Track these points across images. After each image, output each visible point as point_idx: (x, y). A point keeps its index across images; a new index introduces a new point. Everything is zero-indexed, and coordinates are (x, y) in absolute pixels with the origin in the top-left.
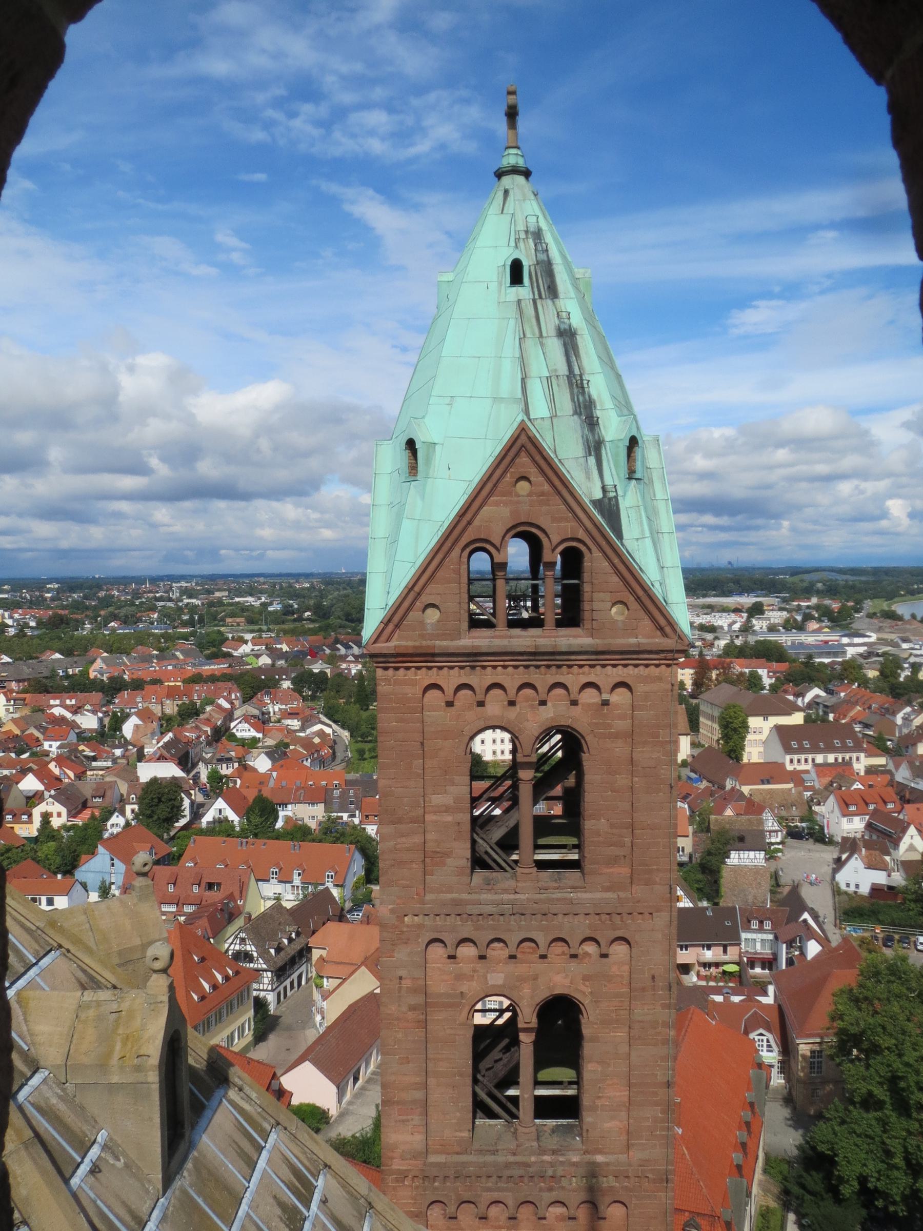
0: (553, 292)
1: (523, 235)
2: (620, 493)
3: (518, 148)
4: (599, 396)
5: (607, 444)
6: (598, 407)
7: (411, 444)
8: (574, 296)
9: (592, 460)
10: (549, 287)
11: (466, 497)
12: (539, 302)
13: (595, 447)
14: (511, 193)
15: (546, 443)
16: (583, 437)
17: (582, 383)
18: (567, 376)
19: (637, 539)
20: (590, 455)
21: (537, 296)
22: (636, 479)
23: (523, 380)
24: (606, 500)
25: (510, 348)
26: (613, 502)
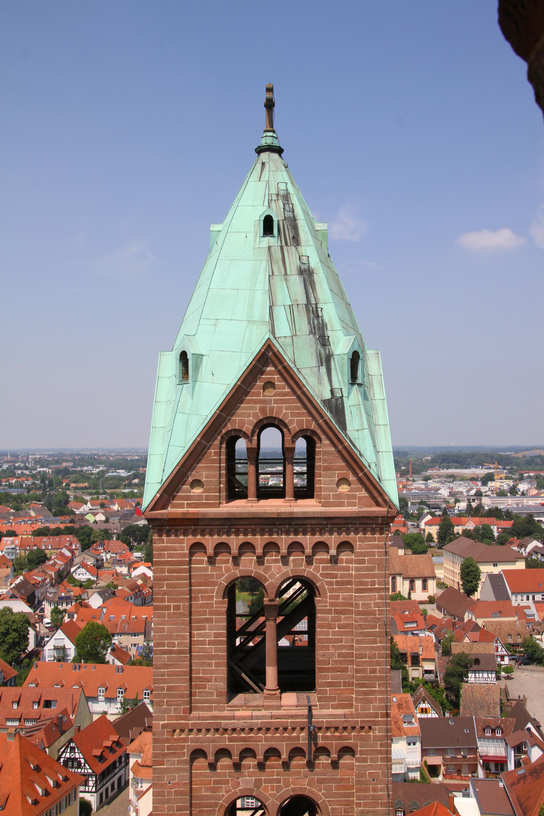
0: (296, 240)
1: (274, 197)
2: (345, 394)
3: (274, 132)
4: (330, 320)
5: (336, 357)
6: (329, 328)
7: (184, 356)
8: (312, 243)
9: (323, 369)
10: (293, 238)
11: (225, 396)
12: (285, 248)
14: (267, 165)
15: (287, 356)
16: (316, 352)
17: (317, 311)
18: (305, 305)
19: (358, 430)
20: (322, 365)
21: (284, 244)
22: (358, 384)
23: (271, 307)
24: (334, 400)
25: (262, 284)
26: (339, 401)
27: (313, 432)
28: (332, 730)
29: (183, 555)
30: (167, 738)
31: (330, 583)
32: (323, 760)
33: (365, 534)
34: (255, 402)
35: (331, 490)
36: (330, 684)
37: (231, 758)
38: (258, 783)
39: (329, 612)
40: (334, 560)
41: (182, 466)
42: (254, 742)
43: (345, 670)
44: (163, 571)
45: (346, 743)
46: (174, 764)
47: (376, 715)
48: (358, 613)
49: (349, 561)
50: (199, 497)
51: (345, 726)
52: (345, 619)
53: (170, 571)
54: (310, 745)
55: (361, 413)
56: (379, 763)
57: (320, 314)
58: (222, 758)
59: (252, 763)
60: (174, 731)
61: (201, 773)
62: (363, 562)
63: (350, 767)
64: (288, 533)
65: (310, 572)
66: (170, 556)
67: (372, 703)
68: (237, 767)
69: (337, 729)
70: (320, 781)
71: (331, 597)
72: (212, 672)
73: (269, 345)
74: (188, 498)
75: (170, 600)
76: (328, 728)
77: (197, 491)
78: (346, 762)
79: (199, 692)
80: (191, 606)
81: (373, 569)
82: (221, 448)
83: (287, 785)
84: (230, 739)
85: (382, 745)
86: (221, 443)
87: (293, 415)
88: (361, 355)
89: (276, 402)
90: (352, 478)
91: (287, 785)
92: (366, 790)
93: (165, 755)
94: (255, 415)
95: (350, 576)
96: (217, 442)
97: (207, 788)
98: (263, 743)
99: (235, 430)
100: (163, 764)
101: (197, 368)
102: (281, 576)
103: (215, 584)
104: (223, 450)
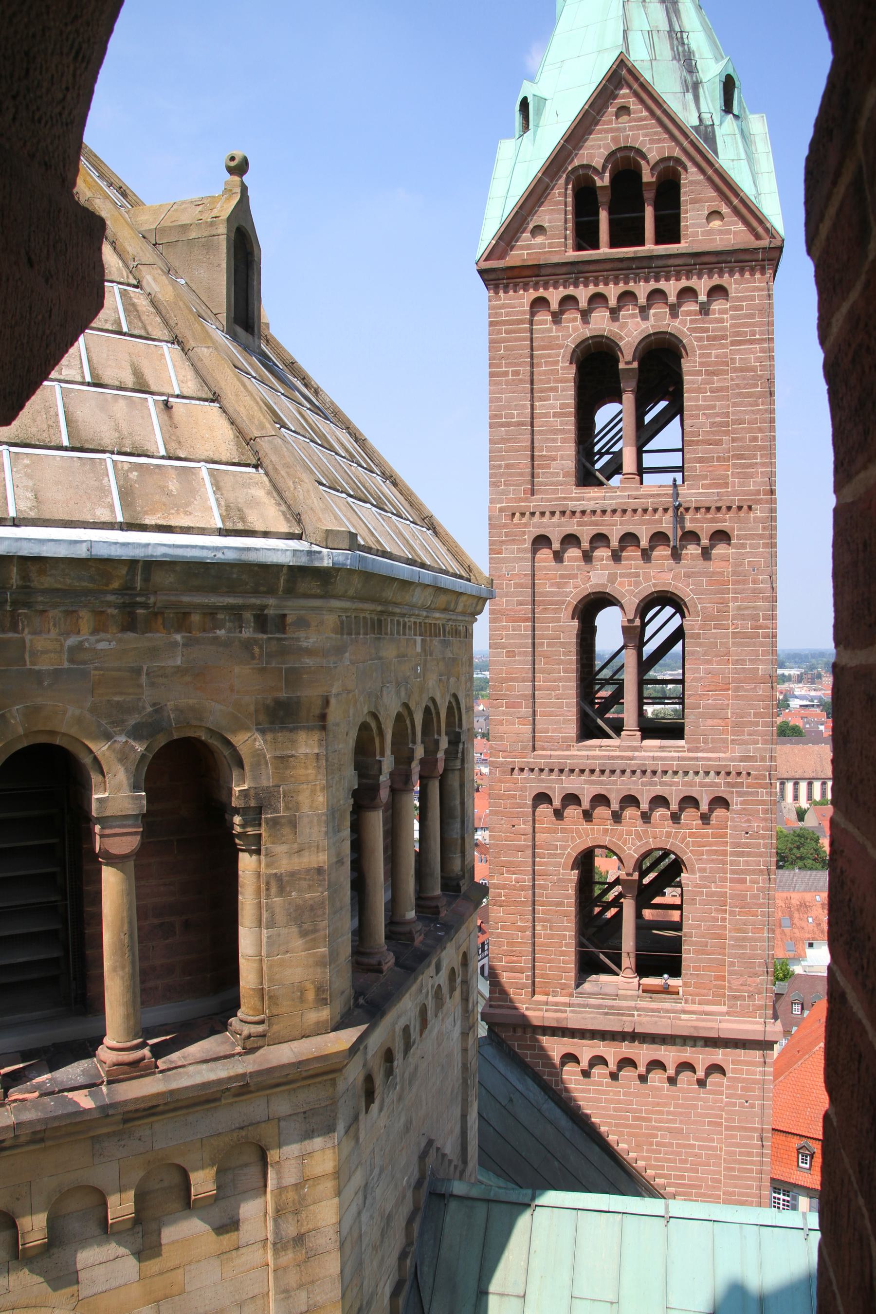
2: (717, 122)
4: (698, 47)
5: (705, 85)
6: (697, 56)
9: (690, 96)
13: (695, 87)
16: (681, 78)
17: (682, 38)
18: (668, 32)
19: (733, 160)
20: (688, 91)
22: (734, 115)
23: (625, 32)
24: (702, 128)
26: (710, 129)
27: (678, 161)
28: (703, 510)
29: (524, 313)
30: (505, 523)
31: (700, 339)
32: (693, 550)
33: (742, 275)
34: (607, 131)
35: (700, 226)
36: (701, 460)
37: (580, 548)
38: (612, 578)
39: (699, 373)
40: (704, 310)
41: (521, 208)
42: (607, 525)
43: (719, 442)
44: (500, 332)
45: (719, 526)
46: (513, 553)
47: (758, 492)
48: (736, 370)
49: (722, 312)
50: (542, 246)
51: (719, 505)
52: (719, 381)
53: (507, 332)
54: (675, 528)
55: (737, 143)
56: (761, 550)
57: (686, 41)
58: (570, 548)
59: (605, 554)
60: (514, 514)
61: (544, 566)
62: (740, 308)
63: (725, 558)
64: (647, 280)
65: (675, 327)
66: (507, 314)
67: (753, 478)
68: (587, 557)
69: (708, 509)
70: (688, 575)
71: (702, 356)
72: (558, 449)
73: (622, 61)
74: (528, 247)
75: (508, 365)
76: (697, 509)
77: (539, 239)
78: (719, 553)
79: (543, 473)
80: (532, 373)
81: (753, 316)
82: (566, 189)
83: (646, 579)
84: (579, 524)
85: (764, 528)
86: (567, 184)
87: (652, 142)
88: (737, 83)
89: (631, 129)
90: (725, 209)
91: (646, 579)
92: (745, 582)
93: (502, 542)
94: (606, 146)
95: (724, 329)
96: (562, 181)
97: (552, 583)
98: (619, 527)
99: (582, 166)
101: (539, 112)
102: (640, 333)
103: (560, 347)
104: (570, 192)
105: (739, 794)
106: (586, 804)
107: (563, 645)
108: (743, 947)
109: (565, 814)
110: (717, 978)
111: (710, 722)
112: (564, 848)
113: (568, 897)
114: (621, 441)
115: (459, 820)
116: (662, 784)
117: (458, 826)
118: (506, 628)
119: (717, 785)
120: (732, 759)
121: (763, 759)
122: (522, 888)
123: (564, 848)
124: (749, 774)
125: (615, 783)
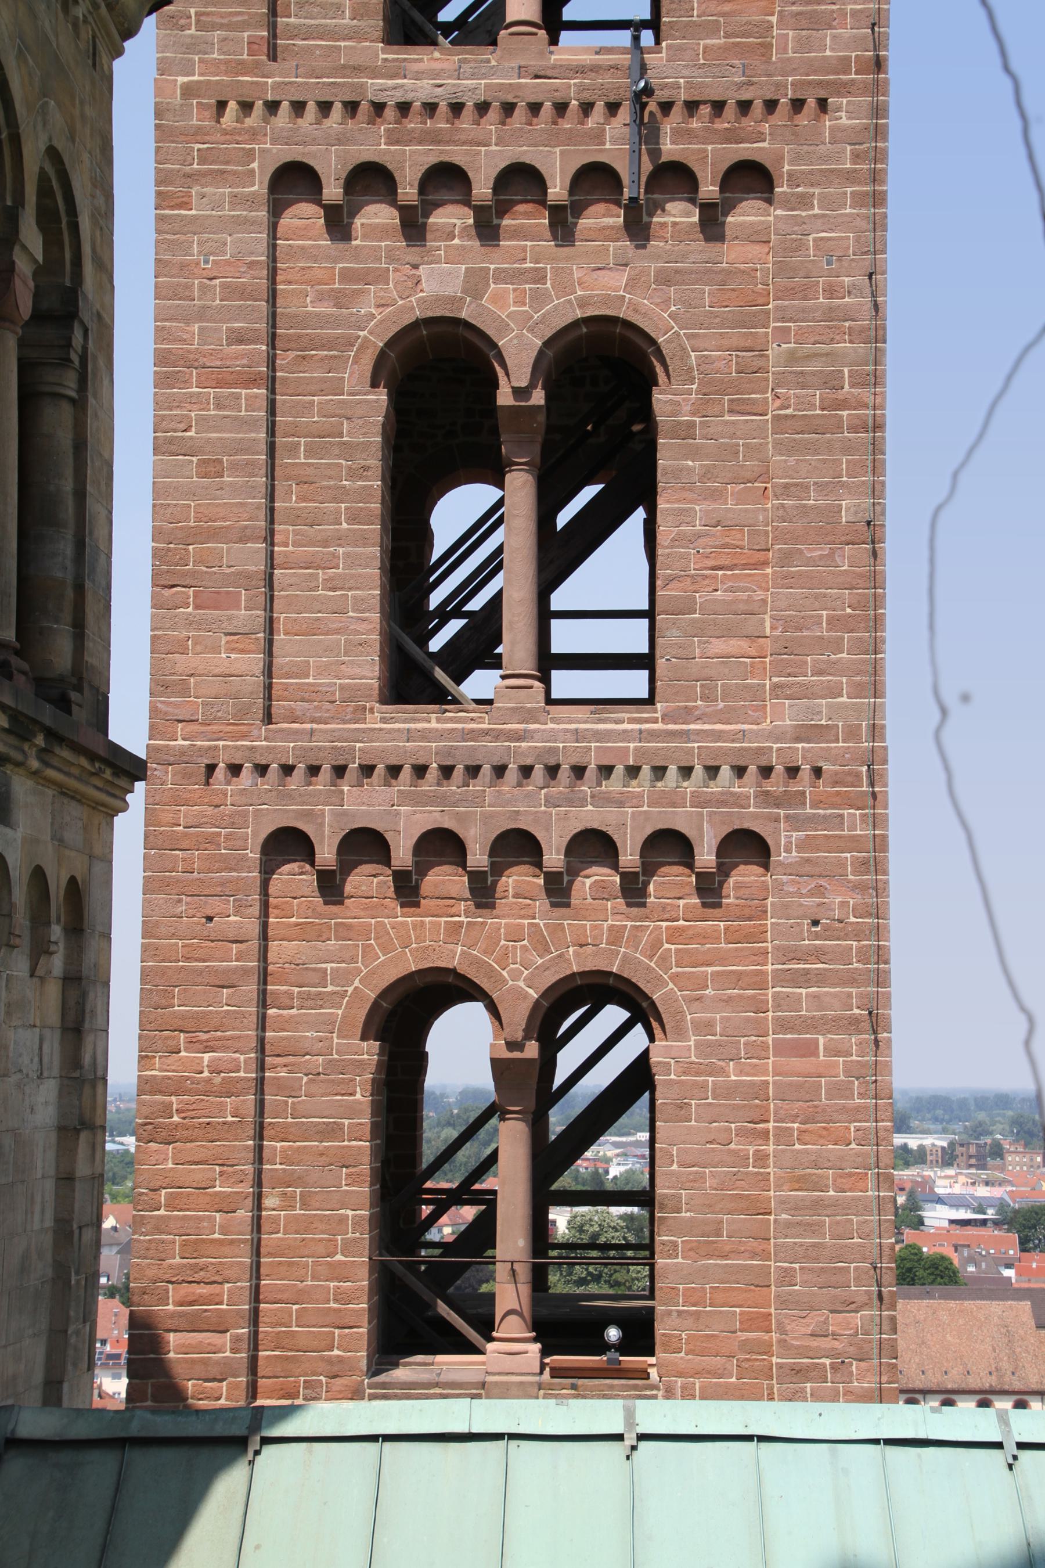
28: (705, 110)
30: (199, 128)
38: (475, 284)
42: (464, 143)
45: (745, 150)
46: (220, 206)
47: (844, 65)
51: (745, 96)
54: (638, 154)
56: (848, 211)
58: (368, 203)
59: (458, 222)
60: (222, 105)
61: (303, 248)
63: (759, 237)
67: (831, 27)
69: (718, 106)
76: (692, 106)
78: (745, 222)
85: (856, 157)
92: (805, 292)
97: (321, 293)
98: (494, 148)
100: (185, 205)
105: (795, 823)
106: (402, 854)
107: (348, 450)
108: (814, 1229)
109: (348, 889)
110: (751, 1322)
111: (718, 646)
112: (342, 978)
113: (351, 1112)
114: (502, 529)
115: (69, 534)
116: (598, 799)
117: (66, 547)
118: (195, 400)
119: (740, 801)
120: (777, 736)
121: (852, 733)
122: (229, 1090)
123: (342, 978)
124: (817, 772)
125: (478, 800)
